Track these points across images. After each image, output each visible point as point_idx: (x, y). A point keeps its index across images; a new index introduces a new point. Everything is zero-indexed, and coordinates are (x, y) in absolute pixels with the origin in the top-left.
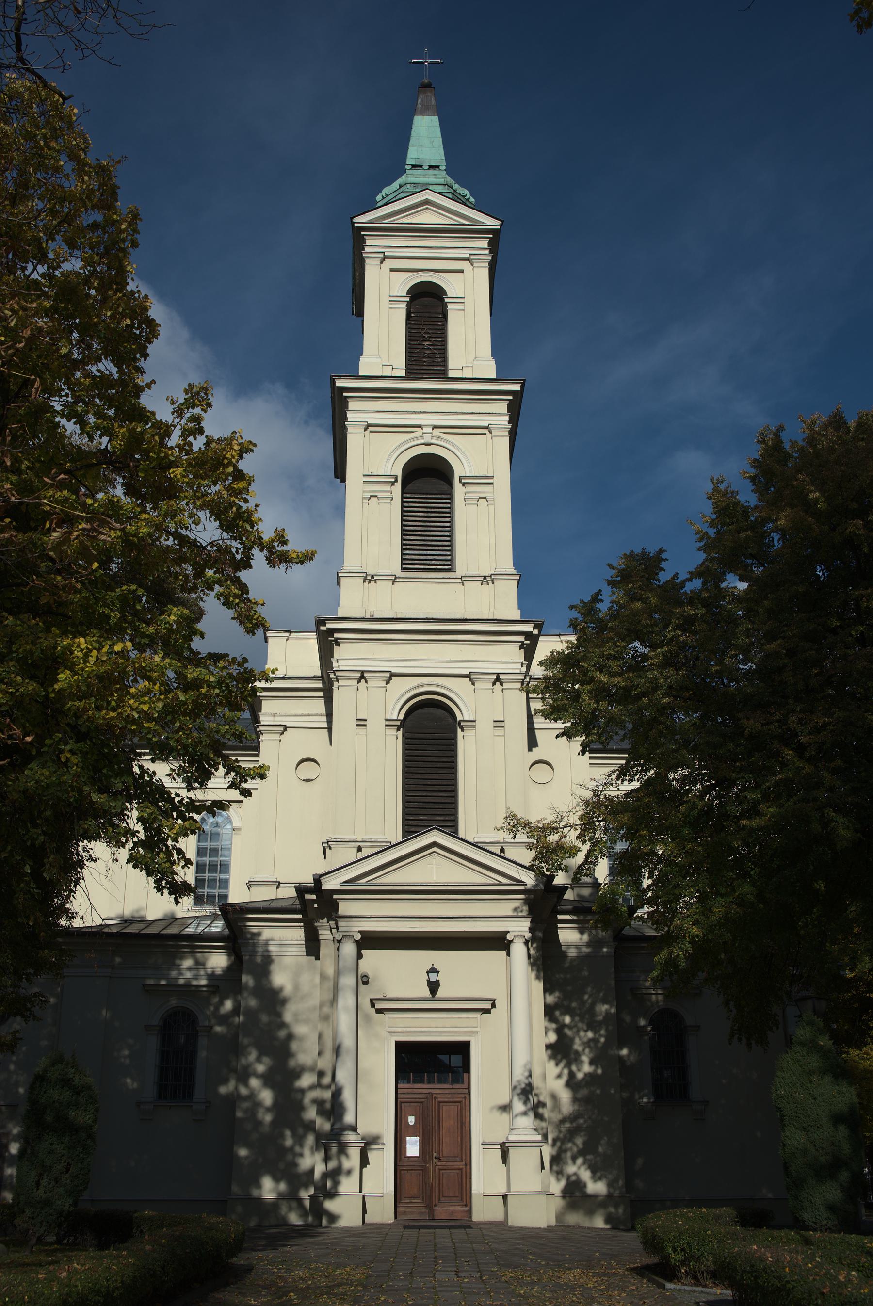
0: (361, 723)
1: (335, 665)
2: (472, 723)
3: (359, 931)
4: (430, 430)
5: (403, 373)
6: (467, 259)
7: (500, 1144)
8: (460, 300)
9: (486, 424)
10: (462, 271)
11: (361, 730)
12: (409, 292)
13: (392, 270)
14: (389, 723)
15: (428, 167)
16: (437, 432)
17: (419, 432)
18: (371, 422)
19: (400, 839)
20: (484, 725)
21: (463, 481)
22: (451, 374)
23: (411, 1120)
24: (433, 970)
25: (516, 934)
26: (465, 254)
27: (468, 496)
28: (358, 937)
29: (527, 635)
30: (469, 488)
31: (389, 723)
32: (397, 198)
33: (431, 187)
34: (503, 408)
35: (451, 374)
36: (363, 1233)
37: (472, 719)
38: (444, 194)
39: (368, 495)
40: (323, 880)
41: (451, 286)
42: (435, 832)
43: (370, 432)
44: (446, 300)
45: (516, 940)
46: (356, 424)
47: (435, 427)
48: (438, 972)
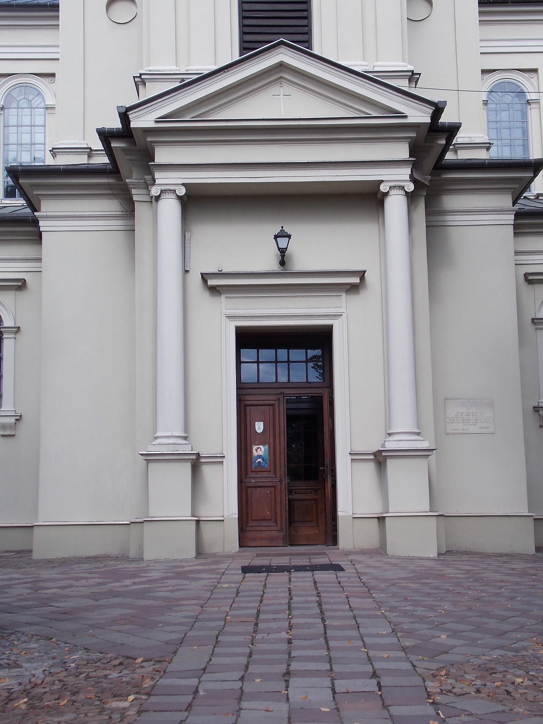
3: (183, 184)
7: (374, 454)
19: (237, 57)
23: (259, 427)
24: (283, 235)
25: (392, 184)
28: (182, 191)
36: (190, 572)
40: (132, 115)
42: (283, 49)
45: (392, 192)
48: (289, 237)
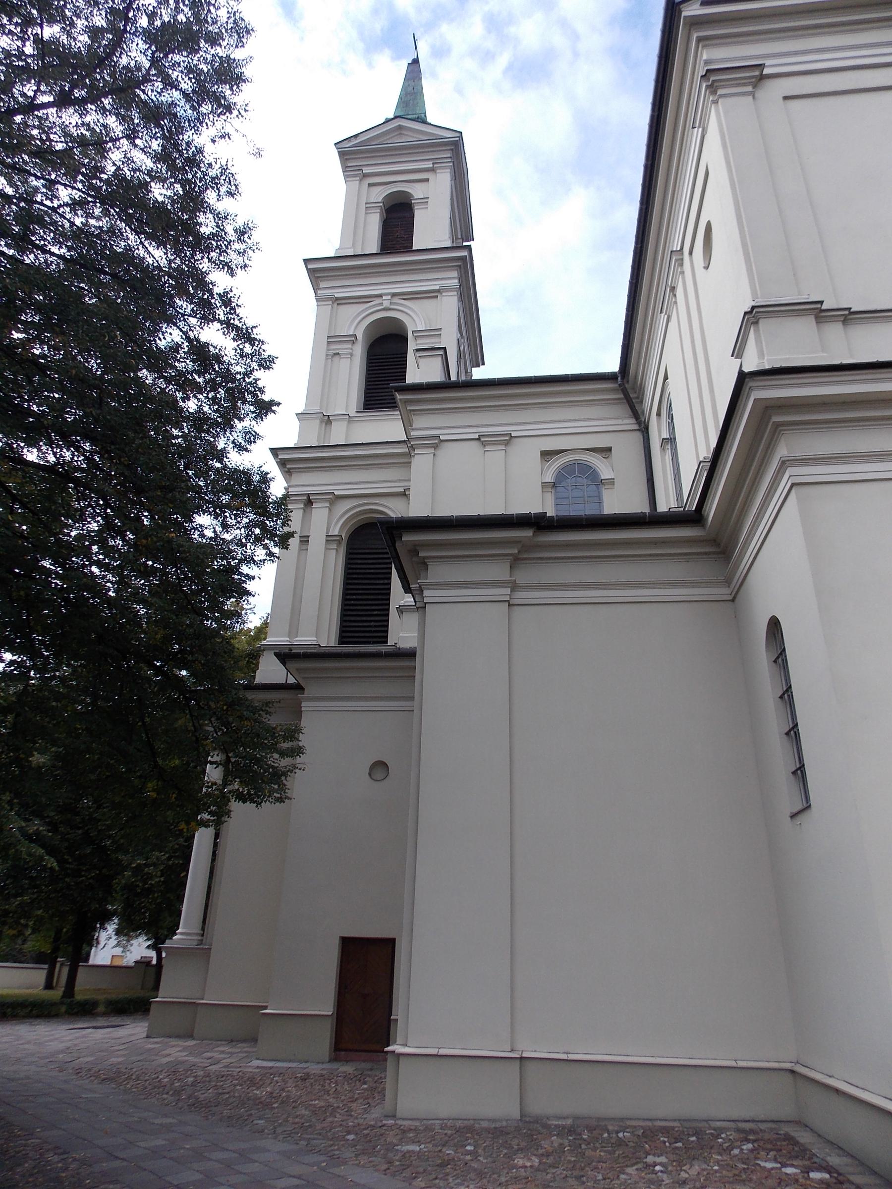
4: (389, 297)
8: (425, 201)
9: (437, 287)
10: (427, 180)
11: (304, 547)
14: (330, 539)
16: (396, 300)
17: (378, 301)
26: (429, 165)
39: (331, 352)
41: (417, 192)
43: (338, 304)
44: (413, 202)
47: (394, 295)
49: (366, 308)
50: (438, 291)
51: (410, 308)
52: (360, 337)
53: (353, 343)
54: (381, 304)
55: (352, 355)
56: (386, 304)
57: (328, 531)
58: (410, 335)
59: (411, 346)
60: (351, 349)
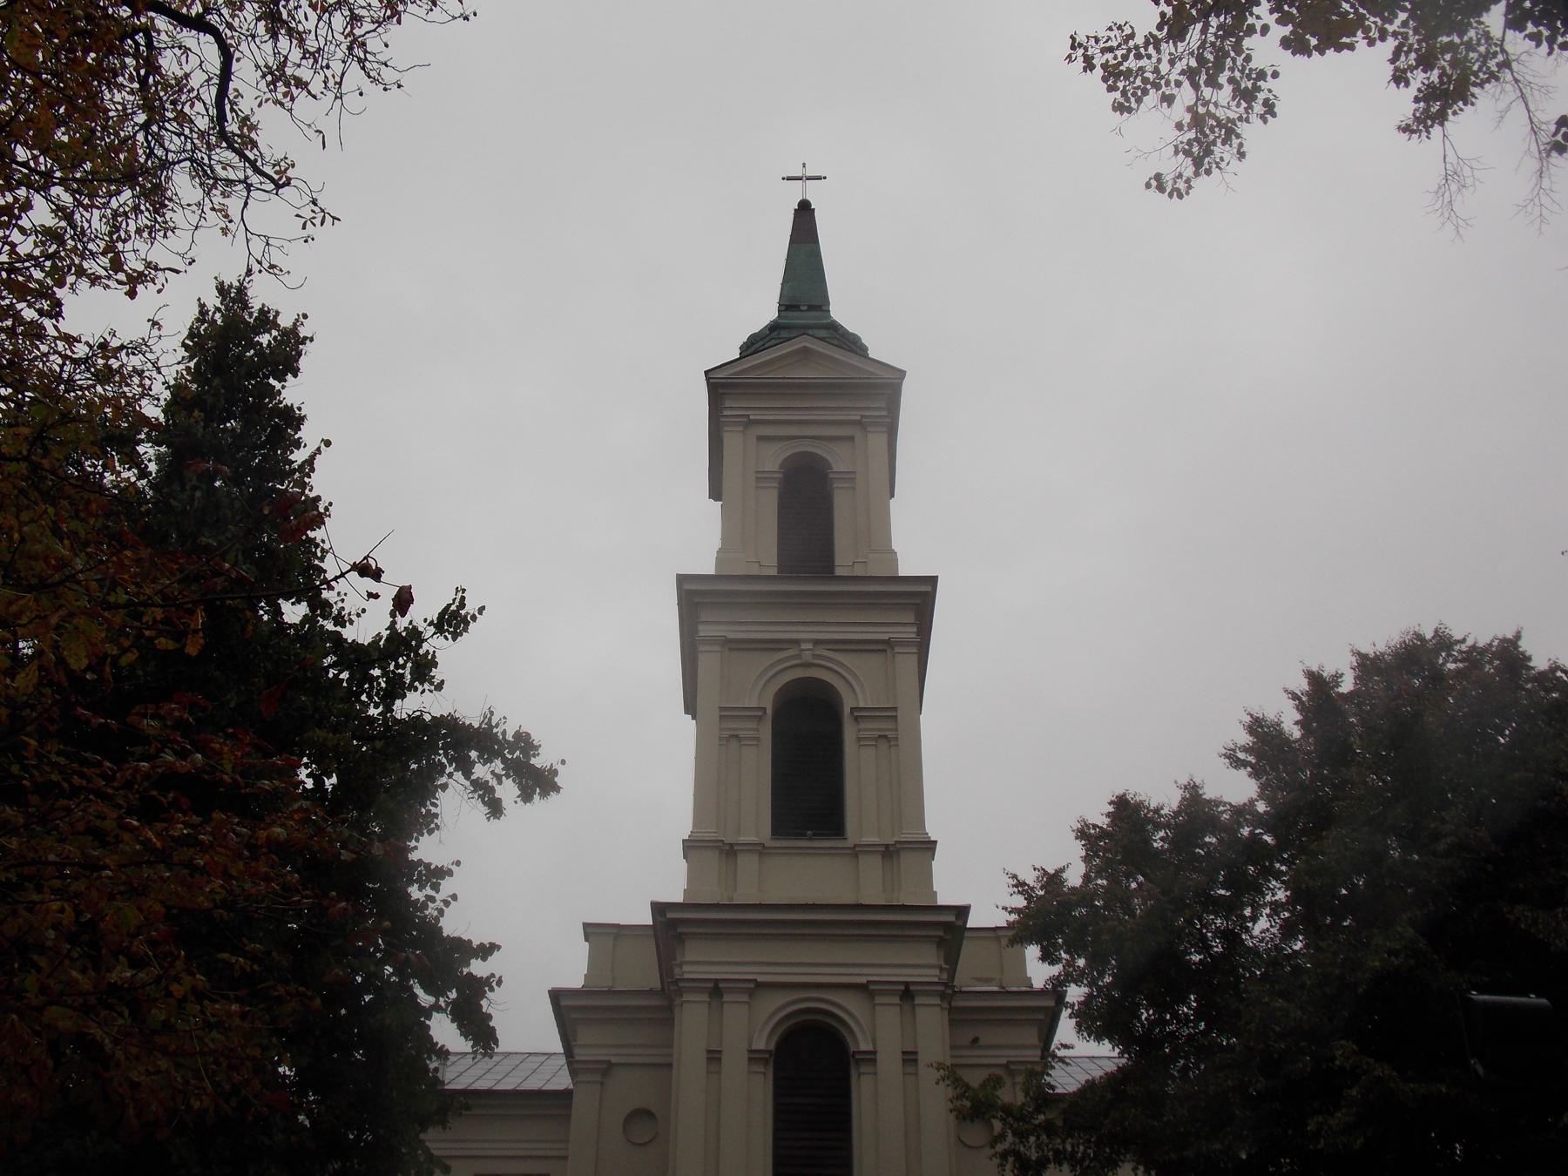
0: (714, 1057)
1: (677, 971)
2: (871, 1058)
5: (774, 572)
6: (859, 423)
8: (850, 477)
9: (885, 637)
10: (851, 439)
12: (781, 466)
13: (760, 438)
14: (755, 1057)
15: (806, 308)
18: (731, 636)
20: (889, 1061)
21: (856, 714)
22: (839, 572)
27: (863, 734)
29: (947, 926)
30: (863, 725)
31: (755, 1057)
32: (766, 346)
33: (810, 332)
34: (910, 617)
35: (839, 572)
37: (871, 1048)
38: (827, 340)
39: (726, 734)
44: (831, 476)
46: (711, 641)
47: (817, 642)
49: (780, 660)
50: (887, 642)
51: (842, 665)
52: (769, 711)
53: (760, 719)
54: (798, 656)
55: (758, 739)
56: (807, 657)
57: (750, 1045)
58: (847, 710)
59: (850, 732)
60: (757, 730)
